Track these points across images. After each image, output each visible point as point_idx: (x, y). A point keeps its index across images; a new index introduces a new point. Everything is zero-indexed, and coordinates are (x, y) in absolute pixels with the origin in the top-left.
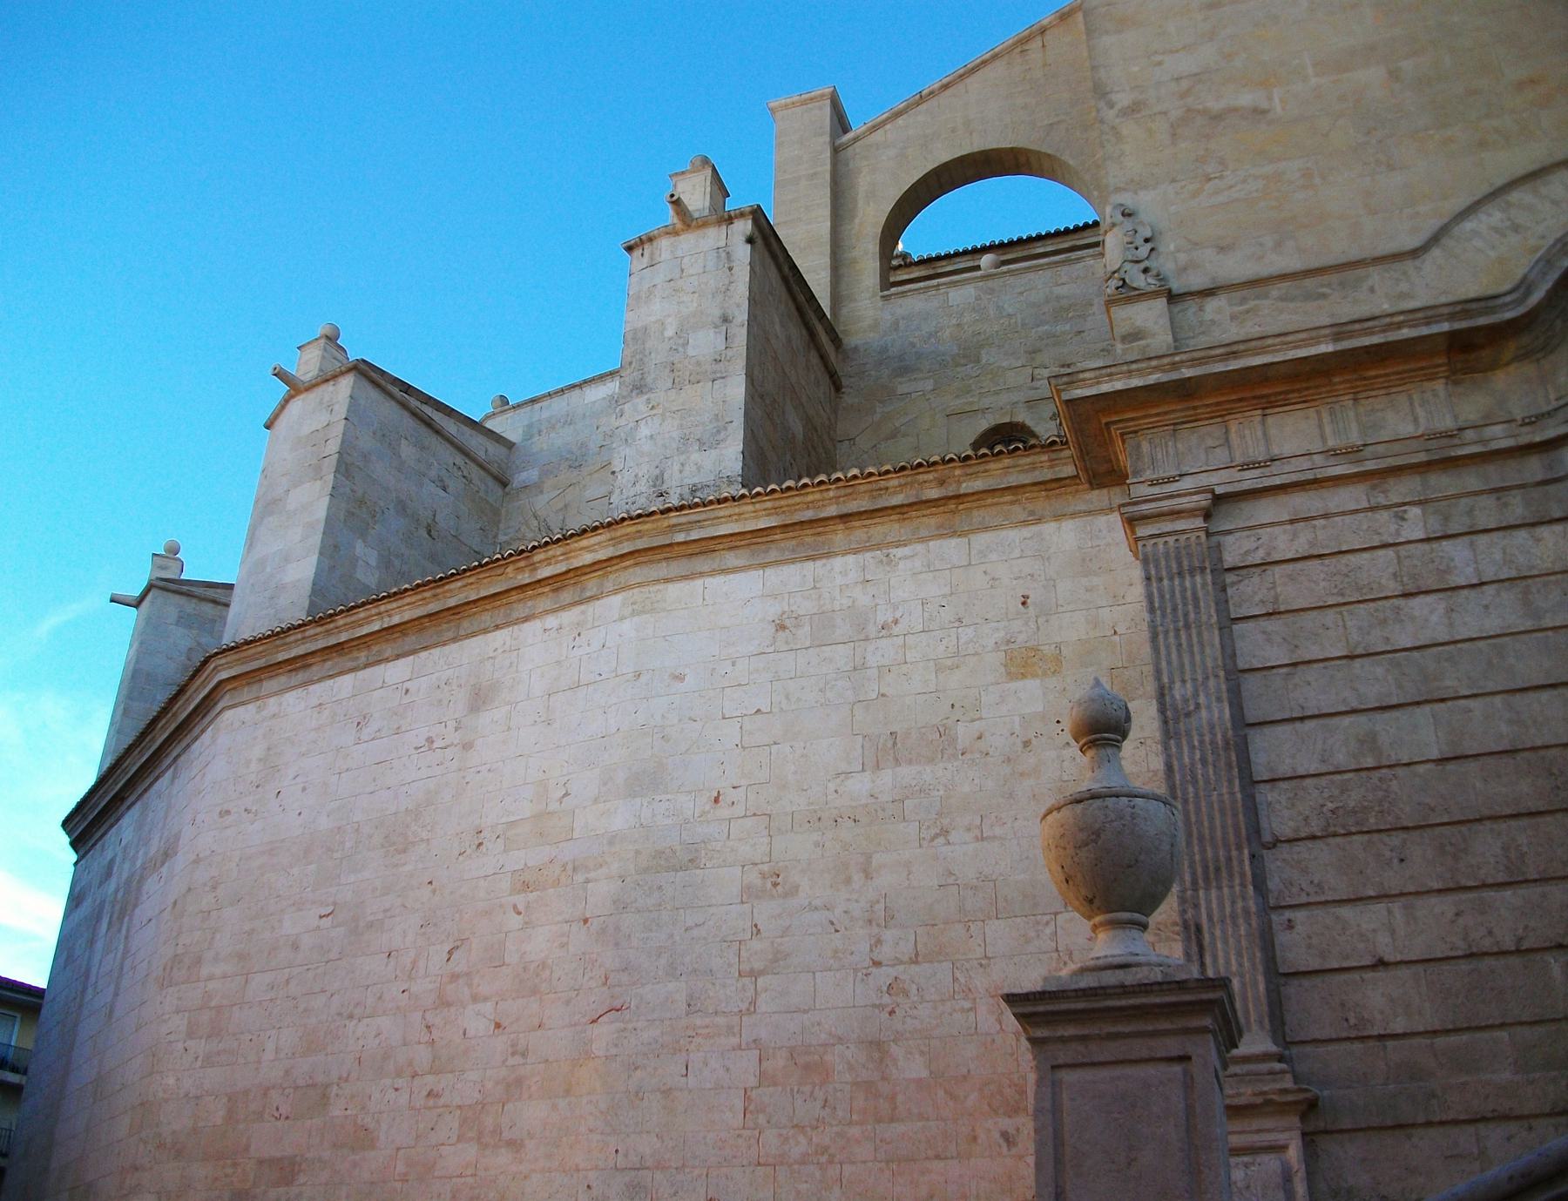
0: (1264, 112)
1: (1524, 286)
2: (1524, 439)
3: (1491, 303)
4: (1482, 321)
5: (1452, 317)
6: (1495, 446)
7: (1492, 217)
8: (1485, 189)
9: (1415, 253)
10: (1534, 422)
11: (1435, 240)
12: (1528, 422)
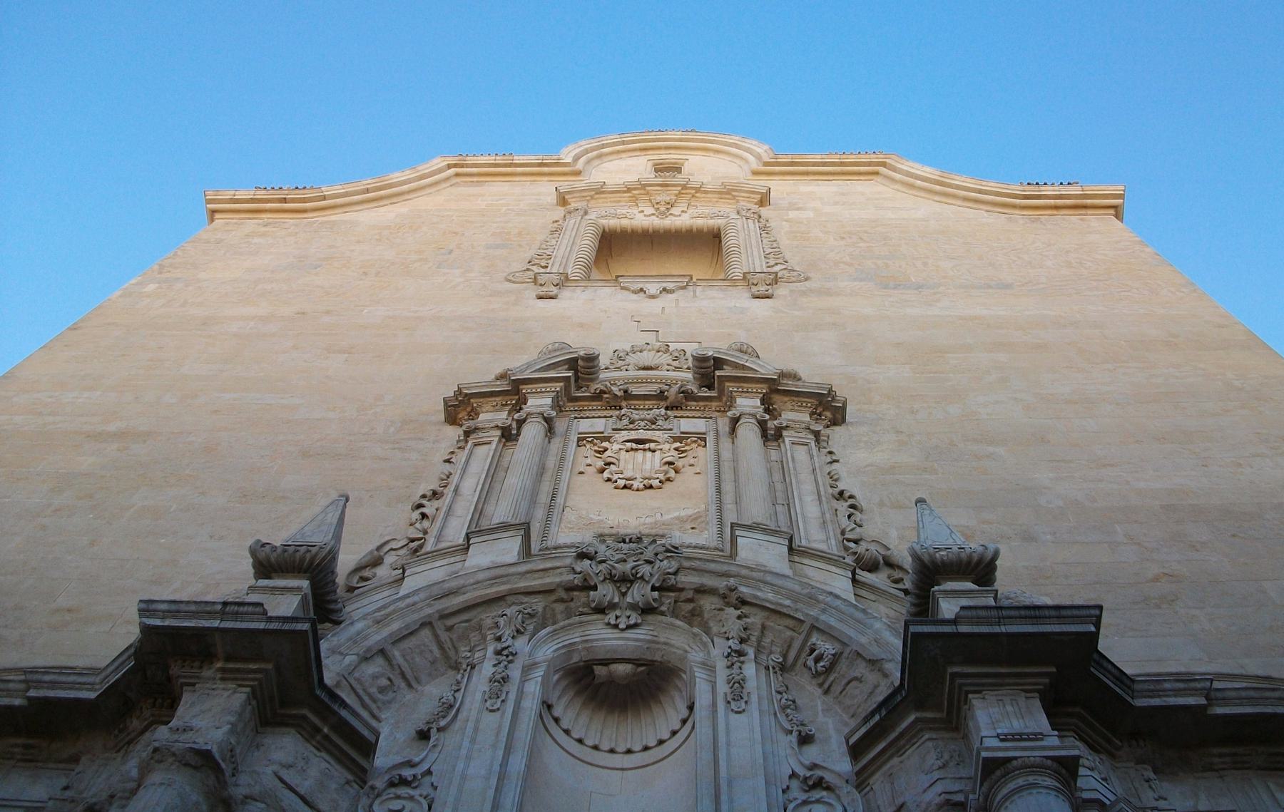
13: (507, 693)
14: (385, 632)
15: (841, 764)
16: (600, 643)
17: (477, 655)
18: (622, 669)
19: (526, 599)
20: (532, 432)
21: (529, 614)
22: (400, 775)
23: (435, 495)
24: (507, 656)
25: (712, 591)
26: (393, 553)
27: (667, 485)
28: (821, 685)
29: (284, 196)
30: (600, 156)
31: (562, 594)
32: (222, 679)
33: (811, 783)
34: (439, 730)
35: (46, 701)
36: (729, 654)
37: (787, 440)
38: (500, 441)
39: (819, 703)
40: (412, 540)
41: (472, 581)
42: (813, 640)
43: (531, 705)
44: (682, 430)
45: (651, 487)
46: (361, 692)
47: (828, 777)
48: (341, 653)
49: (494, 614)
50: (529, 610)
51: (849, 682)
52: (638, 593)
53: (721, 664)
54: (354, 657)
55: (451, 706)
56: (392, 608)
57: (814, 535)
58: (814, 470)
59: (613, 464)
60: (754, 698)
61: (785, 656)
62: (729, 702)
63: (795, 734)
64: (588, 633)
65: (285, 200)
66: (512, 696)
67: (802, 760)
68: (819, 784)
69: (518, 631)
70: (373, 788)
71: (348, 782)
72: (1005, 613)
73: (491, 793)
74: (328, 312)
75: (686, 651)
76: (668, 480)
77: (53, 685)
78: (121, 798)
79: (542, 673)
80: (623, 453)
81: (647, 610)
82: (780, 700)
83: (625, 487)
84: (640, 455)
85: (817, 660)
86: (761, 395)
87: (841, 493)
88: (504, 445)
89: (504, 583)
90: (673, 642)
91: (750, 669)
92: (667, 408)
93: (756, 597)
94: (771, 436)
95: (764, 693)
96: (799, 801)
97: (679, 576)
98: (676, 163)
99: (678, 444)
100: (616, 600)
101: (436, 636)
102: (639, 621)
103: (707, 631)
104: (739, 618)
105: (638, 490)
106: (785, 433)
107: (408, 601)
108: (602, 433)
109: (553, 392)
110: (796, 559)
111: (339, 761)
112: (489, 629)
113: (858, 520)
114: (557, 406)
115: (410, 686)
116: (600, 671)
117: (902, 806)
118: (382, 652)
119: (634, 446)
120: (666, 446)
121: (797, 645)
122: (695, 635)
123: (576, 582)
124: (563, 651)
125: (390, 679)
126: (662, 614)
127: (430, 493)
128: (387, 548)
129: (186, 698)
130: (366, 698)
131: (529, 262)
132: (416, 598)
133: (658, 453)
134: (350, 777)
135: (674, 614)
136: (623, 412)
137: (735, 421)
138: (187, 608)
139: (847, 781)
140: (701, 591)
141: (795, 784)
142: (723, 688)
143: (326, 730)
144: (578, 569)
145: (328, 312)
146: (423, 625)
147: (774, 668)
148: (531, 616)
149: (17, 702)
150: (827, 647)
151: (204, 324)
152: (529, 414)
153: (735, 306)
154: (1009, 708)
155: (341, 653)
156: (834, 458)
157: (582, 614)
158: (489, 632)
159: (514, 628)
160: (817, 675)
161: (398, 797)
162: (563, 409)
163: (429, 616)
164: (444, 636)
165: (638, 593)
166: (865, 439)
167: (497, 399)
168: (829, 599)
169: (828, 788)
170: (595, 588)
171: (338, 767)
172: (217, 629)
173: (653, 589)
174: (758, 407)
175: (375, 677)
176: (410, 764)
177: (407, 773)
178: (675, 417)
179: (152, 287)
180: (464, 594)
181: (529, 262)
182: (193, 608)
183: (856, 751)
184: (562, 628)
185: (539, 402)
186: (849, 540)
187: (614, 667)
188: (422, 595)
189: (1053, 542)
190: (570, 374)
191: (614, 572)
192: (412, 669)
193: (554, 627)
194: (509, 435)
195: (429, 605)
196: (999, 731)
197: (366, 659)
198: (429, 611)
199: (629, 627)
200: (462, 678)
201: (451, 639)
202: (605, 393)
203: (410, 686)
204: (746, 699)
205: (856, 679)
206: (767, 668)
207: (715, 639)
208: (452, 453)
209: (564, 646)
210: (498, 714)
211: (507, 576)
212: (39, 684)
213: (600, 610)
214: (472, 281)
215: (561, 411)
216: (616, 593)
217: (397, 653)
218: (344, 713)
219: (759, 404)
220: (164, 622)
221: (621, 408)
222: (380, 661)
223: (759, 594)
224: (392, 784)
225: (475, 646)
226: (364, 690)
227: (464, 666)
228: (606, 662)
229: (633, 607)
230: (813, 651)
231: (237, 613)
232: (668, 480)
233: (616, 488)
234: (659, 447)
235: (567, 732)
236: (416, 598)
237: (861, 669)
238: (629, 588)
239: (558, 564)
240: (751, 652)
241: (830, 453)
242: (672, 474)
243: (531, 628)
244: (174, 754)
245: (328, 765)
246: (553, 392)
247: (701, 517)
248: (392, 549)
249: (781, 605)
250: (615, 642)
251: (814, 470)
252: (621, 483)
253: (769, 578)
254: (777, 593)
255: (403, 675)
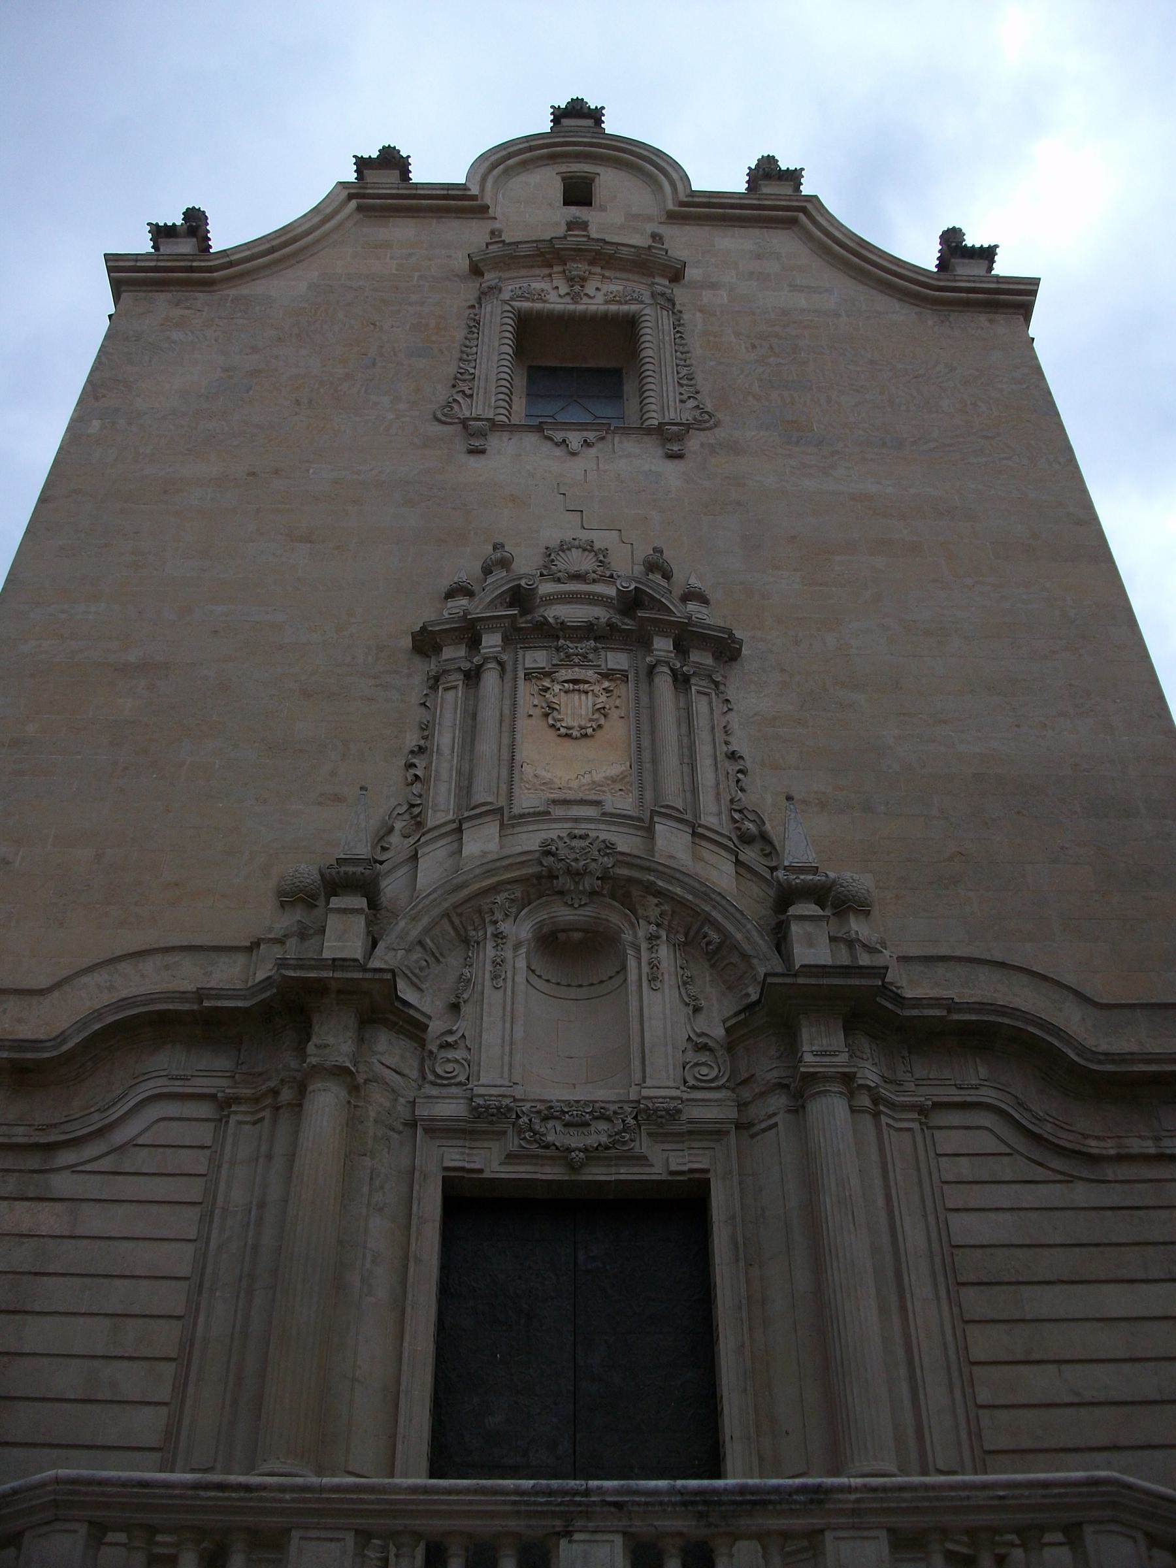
0: (8, 863)
1: (62, 1037)
2: (32, 1140)
3: (40, 1045)
4: (29, 1055)
5: (11, 1049)
6: (14, 1140)
7: (100, 978)
8: (109, 956)
9: (42, 992)
10: (44, 1129)
11: (58, 985)
12: (41, 1129)
13: (506, 972)
14: (420, 926)
15: (719, 1032)
16: (561, 919)
17: (481, 933)
18: (577, 936)
19: (509, 887)
20: (490, 679)
21: (512, 899)
22: (446, 1041)
23: (421, 750)
24: (502, 939)
25: (639, 882)
26: (400, 817)
27: (599, 733)
28: (709, 960)
29: (189, 264)
30: (506, 171)
31: (535, 881)
32: (338, 1004)
33: (700, 1046)
34: (464, 1002)
35: (217, 1007)
36: (649, 939)
37: (693, 688)
38: (463, 683)
39: (707, 975)
40: (413, 806)
41: (471, 876)
42: (706, 929)
43: (521, 978)
44: (609, 667)
45: (586, 735)
46: (410, 975)
47: (711, 1043)
48: (395, 950)
49: (488, 901)
50: (512, 897)
51: (727, 964)
52: (587, 884)
53: (644, 946)
54: (403, 951)
55: (469, 980)
56: (421, 905)
57: (712, 816)
58: (713, 728)
59: (556, 709)
60: (666, 976)
61: (686, 936)
62: (649, 981)
63: (691, 1007)
64: (553, 910)
65: (191, 269)
66: (509, 975)
67: (696, 1029)
68: (705, 1047)
69: (506, 915)
70: (431, 1052)
71: (416, 1048)
72: (827, 970)
73: (506, 1059)
74: (276, 472)
75: (620, 928)
76: (600, 726)
77: (218, 997)
78: (289, 1082)
79: (525, 950)
80: (562, 694)
81: (593, 893)
82: (683, 975)
83: (566, 735)
84: (576, 696)
85: (708, 944)
86: (673, 635)
87: (733, 753)
88: (467, 685)
89: (494, 876)
90: (610, 919)
91: (664, 952)
92: (596, 639)
93: (669, 890)
94: (681, 681)
95: (673, 969)
96: (692, 1064)
97: (615, 868)
98: (586, 178)
99: (606, 684)
100: (572, 888)
101: (452, 923)
102: (588, 901)
103: (634, 912)
104: (657, 905)
105: (576, 738)
106: (693, 681)
107: (431, 897)
108: (544, 668)
109: (500, 627)
110: (697, 841)
111: (410, 1038)
112: (487, 913)
113: (744, 785)
114: (506, 640)
115: (438, 961)
116: (559, 935)
117: (753, 1075)
118: (420, 943)
119: (571, 686)
120: (597, 688)
121: (695, 928)
122: (627, 915)
123: (544, 873)
124: (535, 927)
125: (426, 961)
126: (604, 896)
127: (416, 749)
128: (395, 813)
129: (316, 1019)
130: (414, 979)
131: (454, 386)
132: (435, 896)
133: (590, 694)
134: (416, 1045)
135: (613, 897)
136: (561, 642)
137: (651, 670)
138: (308, 963)
139: (722, 1046)
140: (630, 880)
141: (689, 1046)
142: (645, 969)
143: (401, 1023)
144: (546, 864)
145: (276, 472)
146: (443, 916)
147: (679, 945)
148: (513, 901)
149: (195, 1007)
150: (714, 936)
151: (165, 492)
152: (486, 660)
153: (650, 470)
154: (823, 1028)
155: (395, 950)
156: (730, 707)
157: (548, 895)
158: (486, 916)
159: (503, 913)
160: (707, 953)
161: (448, 1061)
162: (510, 638)
163: (447, 909)
164: (456, 920)
165: (587, 884)
166: (756, 679)
167: (456, 633)
168: (718, 898)
169: (711, 1050)
170: (557, 877)
171: (409, 1041)
172: (330, 978)
173: (598, 878)
174: (671, 652)
175: (417, 962)
176: (451, 1032)
177: (450, 1039)
178: (603, 648)
179: (96, 424)
180: (468, 886)
181: (454, 386)
182: (313, 963)
183: (728, 1030)
184: (536, 907)
185: (491, 641)
186: (735, 810)
187: (571, 934)
188: (439, 892)
189: (885, 813)
190: (516, 612)
191: (570, 868)
192: (438, 948)
193: (530, 907)
194: (473, 677)
195: (446, 899)
196: (814, 1048)
197: (409, 951)
198: (446, 905)
199: (580, 906)
200: (473, 953)
201: (461, 922)
202: (545, 624)
203: (438, 961)
204: (660, 978)
205: (732, 963)
206: (674, 945)
207: (640, 921)
208: (426, 695)
209: (537, 923)
210: (502, 990)
211: (494, 869)
212: (209, 997)
213: (561, 893)
214: (404, 419)
215: (508, 640)
216: (572, 883)
217: (428, 941)
218: (412, 1012)
219: (672, 649)
220: (295, 973)
221: (558, 638)
222: (419, 948)
223: (671, 888)
224: (441, 1047)
225: (478, 925)
226: (412, 973)
227: (473, 943)
228: (563, 931)
229: (583, 892)
230: (705, 937)
231: (343, 966)
232: (600, 726)
233: (559, 736)
234: (591, 688)
235: (539, 977)
236: (435, 896)
237: (735, 959)
238: (580, 879)
239: (530, 858)
240: (663, 934)
241: (727, 701)
242: (602, 721)
243: (514, 910)
244: (326, 1069)
245: (403, 1042)
246: (500, 627)
247: (626, 776)
248: (399, 814)
249: (684, 898)
250: (572, 917)
251: (713, 728)
252: (563, 731)
253: (678, 875)
254: (682, 887)
255: (433, 954)
